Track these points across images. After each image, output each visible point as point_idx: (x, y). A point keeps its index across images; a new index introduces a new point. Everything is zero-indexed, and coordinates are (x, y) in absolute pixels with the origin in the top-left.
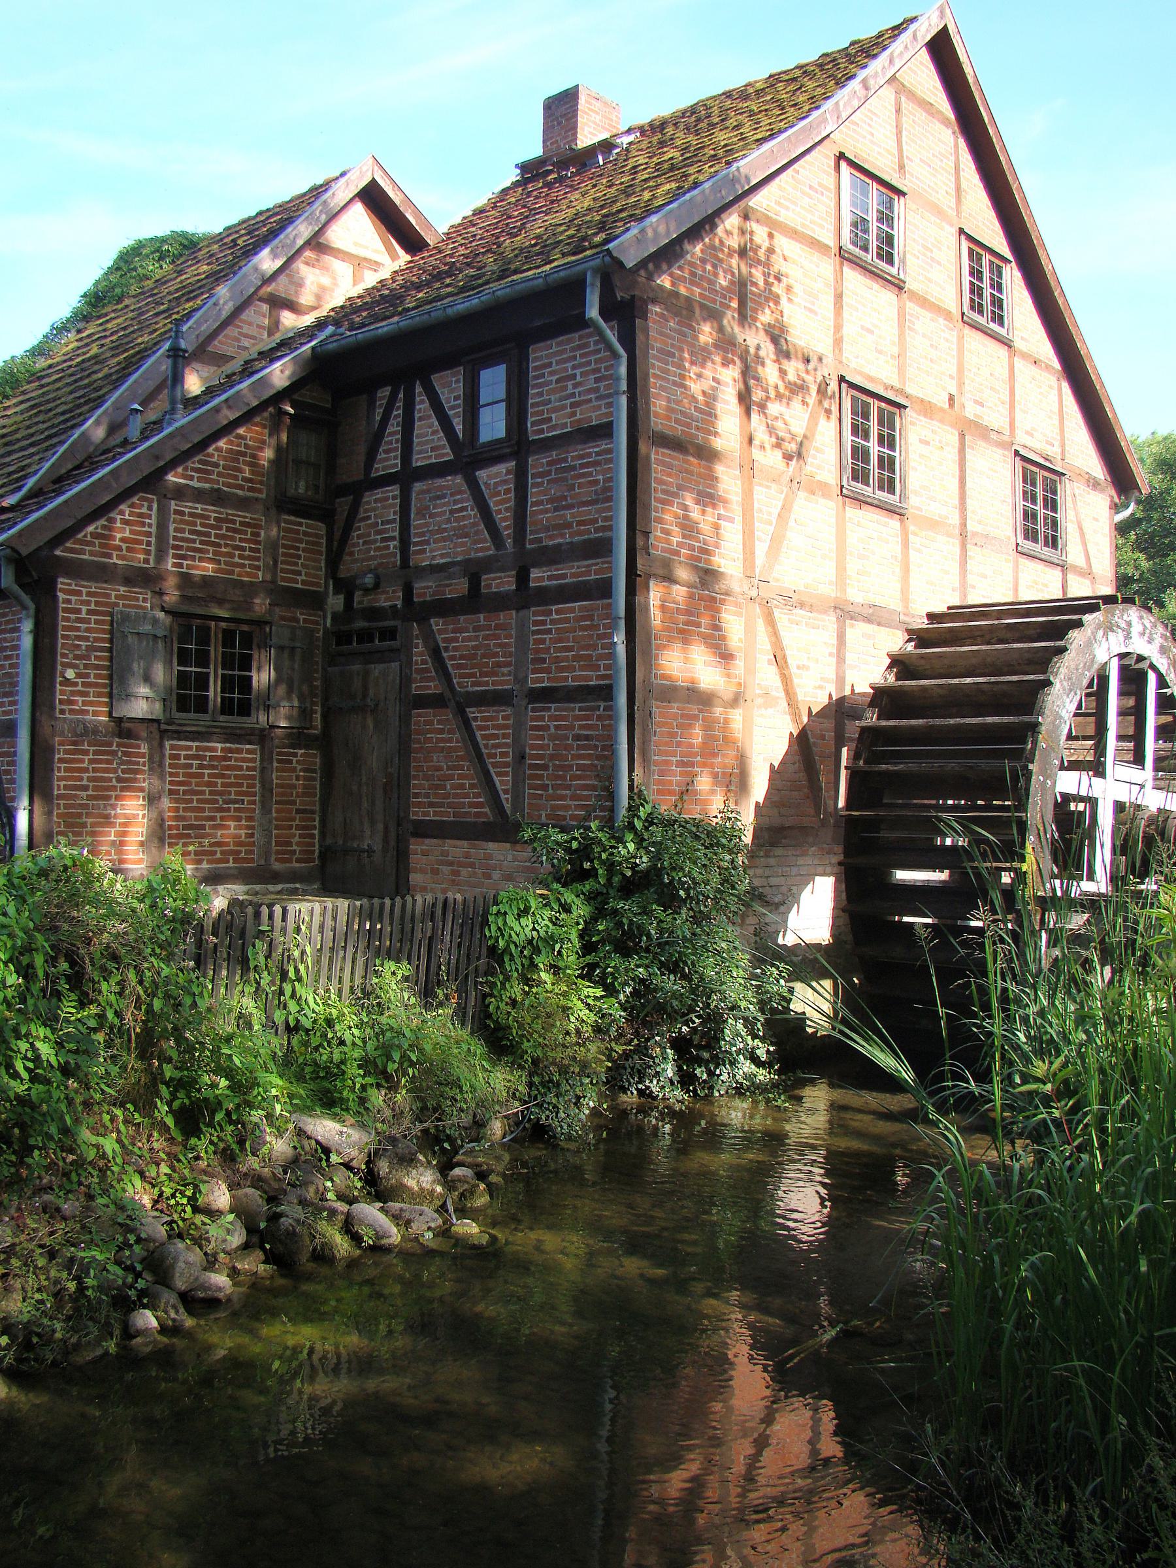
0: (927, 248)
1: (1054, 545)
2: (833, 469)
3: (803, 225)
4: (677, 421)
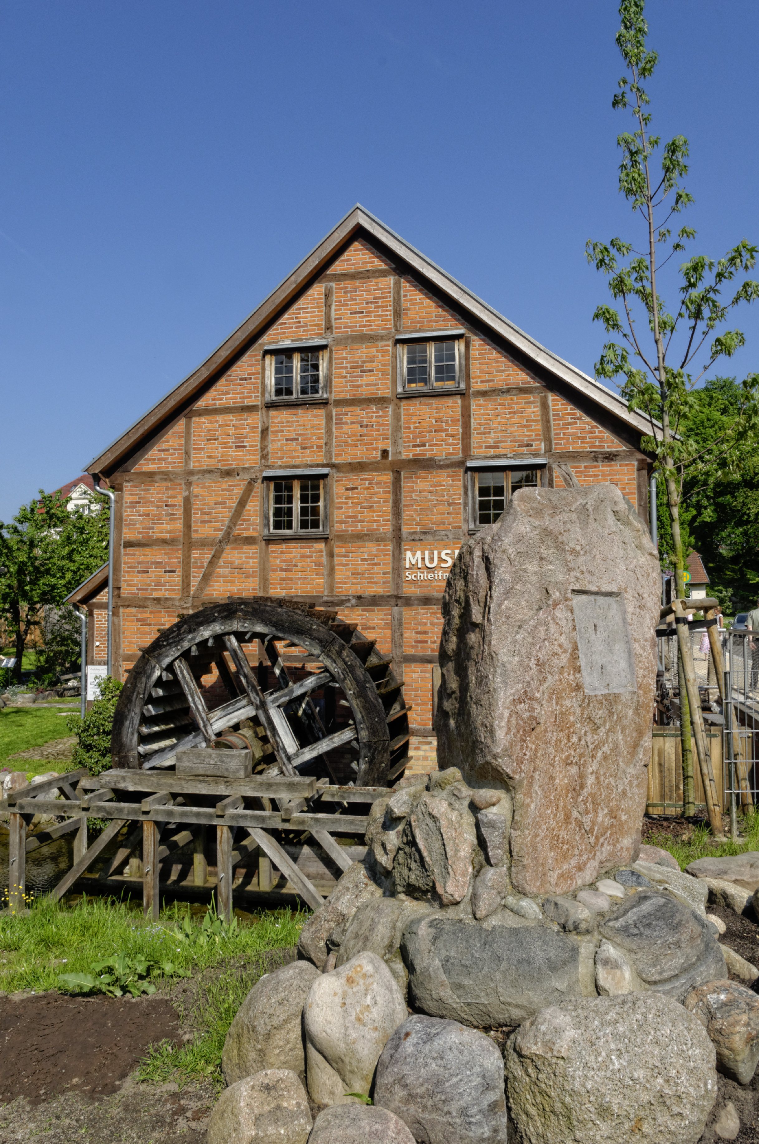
0: (357, 367)
2: (258, 527)
3: (234, 403)
4: (139, 533)
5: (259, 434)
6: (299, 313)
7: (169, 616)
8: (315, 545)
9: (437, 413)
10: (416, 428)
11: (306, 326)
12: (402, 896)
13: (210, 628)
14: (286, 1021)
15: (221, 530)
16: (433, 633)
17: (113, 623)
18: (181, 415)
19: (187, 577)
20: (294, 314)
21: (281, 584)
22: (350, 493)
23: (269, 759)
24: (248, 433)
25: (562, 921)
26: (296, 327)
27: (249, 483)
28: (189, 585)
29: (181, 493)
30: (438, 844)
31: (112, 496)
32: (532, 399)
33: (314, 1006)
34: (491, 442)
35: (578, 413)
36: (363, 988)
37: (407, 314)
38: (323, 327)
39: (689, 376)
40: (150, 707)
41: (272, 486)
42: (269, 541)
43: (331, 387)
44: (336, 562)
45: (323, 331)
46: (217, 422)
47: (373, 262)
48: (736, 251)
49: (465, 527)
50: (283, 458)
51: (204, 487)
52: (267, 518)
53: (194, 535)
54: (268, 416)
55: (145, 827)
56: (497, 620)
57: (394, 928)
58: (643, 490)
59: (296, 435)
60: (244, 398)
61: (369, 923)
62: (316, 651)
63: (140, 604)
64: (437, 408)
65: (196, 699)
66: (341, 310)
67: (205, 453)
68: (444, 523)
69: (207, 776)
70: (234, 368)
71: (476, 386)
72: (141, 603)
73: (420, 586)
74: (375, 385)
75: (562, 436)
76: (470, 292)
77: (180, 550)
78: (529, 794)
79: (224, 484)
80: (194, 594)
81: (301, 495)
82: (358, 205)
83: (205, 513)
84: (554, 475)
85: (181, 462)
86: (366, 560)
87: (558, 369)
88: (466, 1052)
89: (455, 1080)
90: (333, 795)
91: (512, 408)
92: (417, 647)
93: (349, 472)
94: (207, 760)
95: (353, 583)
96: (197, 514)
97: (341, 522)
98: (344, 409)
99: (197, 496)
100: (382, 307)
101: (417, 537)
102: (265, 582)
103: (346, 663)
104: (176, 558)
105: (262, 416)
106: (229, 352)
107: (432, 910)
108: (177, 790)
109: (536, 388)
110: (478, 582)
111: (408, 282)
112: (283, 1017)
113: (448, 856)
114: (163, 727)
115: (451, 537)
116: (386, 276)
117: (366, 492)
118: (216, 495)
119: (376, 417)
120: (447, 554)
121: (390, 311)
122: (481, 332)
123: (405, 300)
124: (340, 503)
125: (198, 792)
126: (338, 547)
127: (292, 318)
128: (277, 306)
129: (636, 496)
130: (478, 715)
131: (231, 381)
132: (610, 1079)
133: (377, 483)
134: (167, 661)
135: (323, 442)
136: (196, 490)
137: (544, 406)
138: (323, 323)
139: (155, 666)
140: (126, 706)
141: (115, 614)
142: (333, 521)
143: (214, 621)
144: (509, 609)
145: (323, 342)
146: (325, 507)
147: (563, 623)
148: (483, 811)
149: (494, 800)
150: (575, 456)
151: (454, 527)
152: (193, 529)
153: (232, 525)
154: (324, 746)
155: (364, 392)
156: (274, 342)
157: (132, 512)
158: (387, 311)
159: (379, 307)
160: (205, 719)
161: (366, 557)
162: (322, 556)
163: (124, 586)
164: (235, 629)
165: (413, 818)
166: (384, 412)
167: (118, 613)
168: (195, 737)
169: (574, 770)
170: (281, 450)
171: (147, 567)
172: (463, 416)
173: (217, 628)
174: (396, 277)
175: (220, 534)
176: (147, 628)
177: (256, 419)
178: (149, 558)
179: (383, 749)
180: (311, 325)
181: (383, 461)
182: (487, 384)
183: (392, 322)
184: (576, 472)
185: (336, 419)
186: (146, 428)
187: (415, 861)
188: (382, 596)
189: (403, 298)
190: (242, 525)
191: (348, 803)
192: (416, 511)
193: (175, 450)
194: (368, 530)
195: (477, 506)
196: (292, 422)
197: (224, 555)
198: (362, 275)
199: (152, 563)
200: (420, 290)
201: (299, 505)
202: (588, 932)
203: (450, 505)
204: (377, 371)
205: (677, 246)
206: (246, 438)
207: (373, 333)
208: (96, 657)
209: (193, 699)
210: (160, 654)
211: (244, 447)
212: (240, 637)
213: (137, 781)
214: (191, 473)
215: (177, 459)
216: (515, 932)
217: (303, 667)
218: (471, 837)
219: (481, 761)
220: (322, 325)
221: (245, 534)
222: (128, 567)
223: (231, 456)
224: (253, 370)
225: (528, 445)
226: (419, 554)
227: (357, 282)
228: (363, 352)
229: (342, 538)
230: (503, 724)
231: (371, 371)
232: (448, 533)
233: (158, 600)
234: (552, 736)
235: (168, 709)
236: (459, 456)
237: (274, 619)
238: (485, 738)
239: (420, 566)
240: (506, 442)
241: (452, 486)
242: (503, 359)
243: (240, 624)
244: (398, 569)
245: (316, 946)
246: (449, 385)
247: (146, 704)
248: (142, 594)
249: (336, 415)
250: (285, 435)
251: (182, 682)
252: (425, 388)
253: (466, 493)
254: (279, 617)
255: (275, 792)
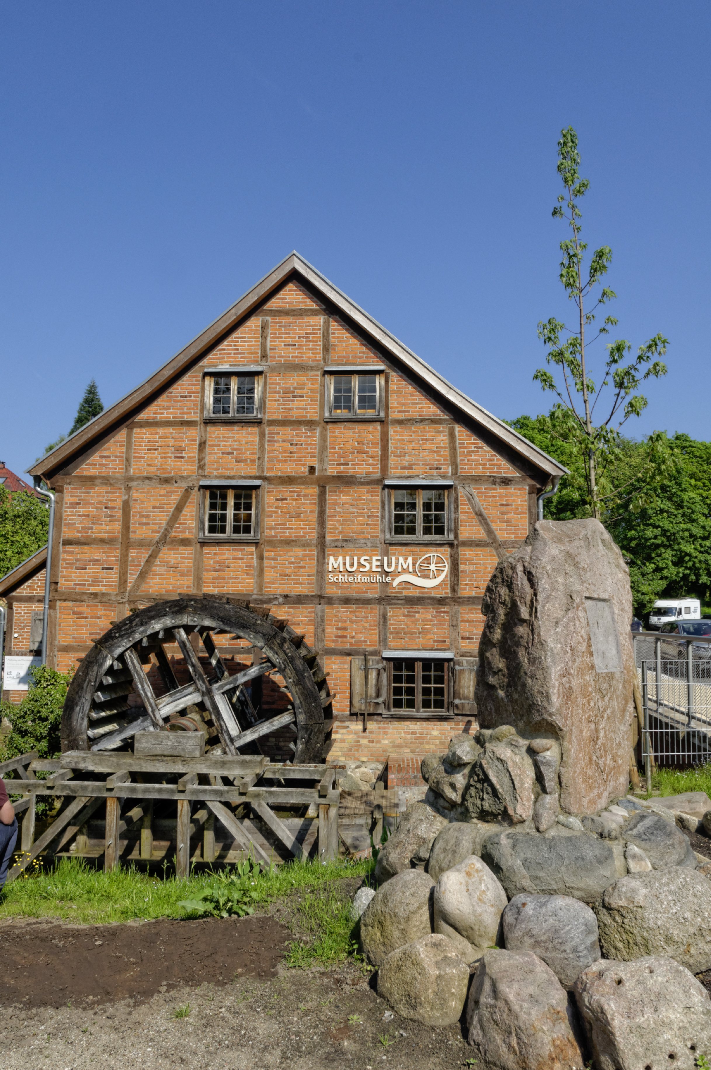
1: (440, 530)
2: (194, 531)
5: (197, 447)
6: (238, 342)
7: (105, 610)
8: (246, 548)
9: (359, 436)
10: (340, 448)
11: (244, 353)
12: (475, 820)
13: (162, 622)
14: (419, 908)
15: (159, 532)
16: (351, 629)
17: (49, 615)
18: (123, 426)
19: (124, 574)
20: (233, 342)
21: (213, 583)
22: (280, 503)
23: (213, 741)
24: (186, 445)
25: (600, 831)
26: (234, 354)
27: (186, 490)
28: (126, 581)
29: (121, 497)
30: (507, 780)
31: (52, 496)
32: (441, 429)
33: (447, 892)
34: (406, 464)
35: (480, 443)
36: (478, 878)
37: (334, 349)
38: (259, 355)
39: (618, 433)
40: (99, 693)
41: (208, 493)
42: (204, 543)
43: (265, 408)
44: (265, 565)
45: (259, 359)
46: (157, 433)
47: (306, 302)
48: (654, 341)
49: (381, 537)
50: (219, 469)
51: (144, 492)
52: (202, 523)
53: (132, 536)
54: (206, 431)
55: (109, 803)
56: (543, 618)
57: (474, 842)
58: (533, 511)
59: (232, 449)
60: (183, 413)
61: (454, 840)
62: (260, 644)
63: (77, 598)
64: (359, 432)
65: (146, 686)
66: (275, 341)
67: (144, 461)
68: (363, 533)
69: (165, 756)
70: (175, 386)
71: (394, 415)
72: (78, 598)
73: (341, 588)
74: (305, 409)
75: (466, 461)
76: (391, 335)
77: (118, 549)
78: (570, 742)
79: (163, 490)
80: (131, 590)
81: (235, 503)
82: (295, 252)
83: (143, 516)
84: (459, 495)
85: (122, 469)
86: (292, 563)
87: (464, 405)
88: (572, 910)
89: (567, 928)
90: (274, 773)
91: (423, 436)
92: (337, 641)
93: (279, 485)
94: (164, 741)
95: (280, 584)
96: (136, 516)
97: (271, 528)
98: (277, 429)
99: (136, 500)
100: (313, 341)
101: (339, 544)
102: (198, 580)
103: (286, 655)
104: (114, 556)
105: (200, 431)
106: (171, 372)
107: (502, 828)
108: (136, 769)
109: (445, 420)
110: (524, 589)
111: (337, 322)
112: (416, 905)
113: (516, 787)
114: (108, 713)
115: (369, 545)
116: (317, 315)
117: (294, 503)
118: (154, 500)
119: (305, 437)
120: (365, 560)
121: (320, 345)
122: (399, 369)
123: (333, 337)
124: (270, 511)
125: (156, 771)
126: (268, 551)
127: (231, 346)
128: (218, 334)
129: (527, 515)
130: (534, 686)
131: (172, 397)
132: (671, 919)
133: (305, 495)
134: (118, 651)
135: (256, 456)
136: (135, 494)
137: (452, 435)
138: (259, 351)
139: (107, 656)
140: (77, 693)
141: (52, 607)
142: (263, 528)
143: (165, 615)
144: (549, 609)
145: (259, 369)
146: (257, 515)
147: (582, 620)
148: (541, 754)
149: (548, 746)
150: (477, 479)
151: (372, 537)
152: (131, 530)
153: (169, 528)
154: (264, 729)
155: (295, 415)
156: (213, 366)
157: (72, 512)
158: (317, 345)
159: (310, 341)
160: (153, 705)
161: (293, 560)
162: (253, 558)
163: (61, 581)
164: (184, 623)
165: (484, 762)
166: (312, 433)
167: (55, 606)
168: (143, 721)
169: (593, 726)
170: (217, 462)
171: (86, 565)
172: (382, 440)
173: (168, 622)
174: (326, 317)
175: (157, 536)
176: (83, 621)
177: (194, 433)
178: (86, 557)
179: (319, 730)
180: (248, 353)
181: (311, 476)
182: (403, 414)
183: (321, 355)
184: (478, 493)
185: (269, 437)
186: (90, 435)
187: (488, 793)
188: (307, 596)
189: (331, 336)
190: (179, 528)
191: (284, 779)
192: (338, 521)
193: (116, 457)
194: (295, 537)
195: (393, 519)
196: (228, 437)
197: (161, 555)
198: (295, 313)
199: (90, 561)
200: (346, 330)
201: (233, 511)
202: (616, 838)
203: (369, 517)
204: (307, 396)
205: (603, 330)
206: (184, 449)
207: (304, 363)
208: (14, 649)
209: (143, 687)
210: (112, 645)
211: (182, 457)
212: (188, 629)
213: (97, 761)
214: (131, 479)
215: (117, 465)
216: (569, 839)
217: (233, 659)
218: (531, 773)
219: (537, 718)
220: (258, 353)
221: (181, 536)
222: (67, 564)
223: (171, 465)
224: (193, 389)
225: (437, 468)
226: (340, 559)
227: (291, 319)
228: (295, 379)
229: (272, 543)
230: (555, 691)
231: (302, 396)
232: (367, 542)
233: (95, 595)
234: (580, 701)
235: (114, 696)
236: (378, 475)
237: (221, 615)
238: (542, 701)
239: (341, 569)
240: (418, 464)
241: (371, 500)
242: (418, 393)
243: (190, 618)
244: (321, 572)
245: (403, 864)
246: (370, 413)
247: (96, 691)
248: (79, 589)
249: (269, 433)
250: (221, 449)
251: (132, 670)
252: (350, 414)
253: (383, 507)
254: (226, 613)
255: (229, 769)
